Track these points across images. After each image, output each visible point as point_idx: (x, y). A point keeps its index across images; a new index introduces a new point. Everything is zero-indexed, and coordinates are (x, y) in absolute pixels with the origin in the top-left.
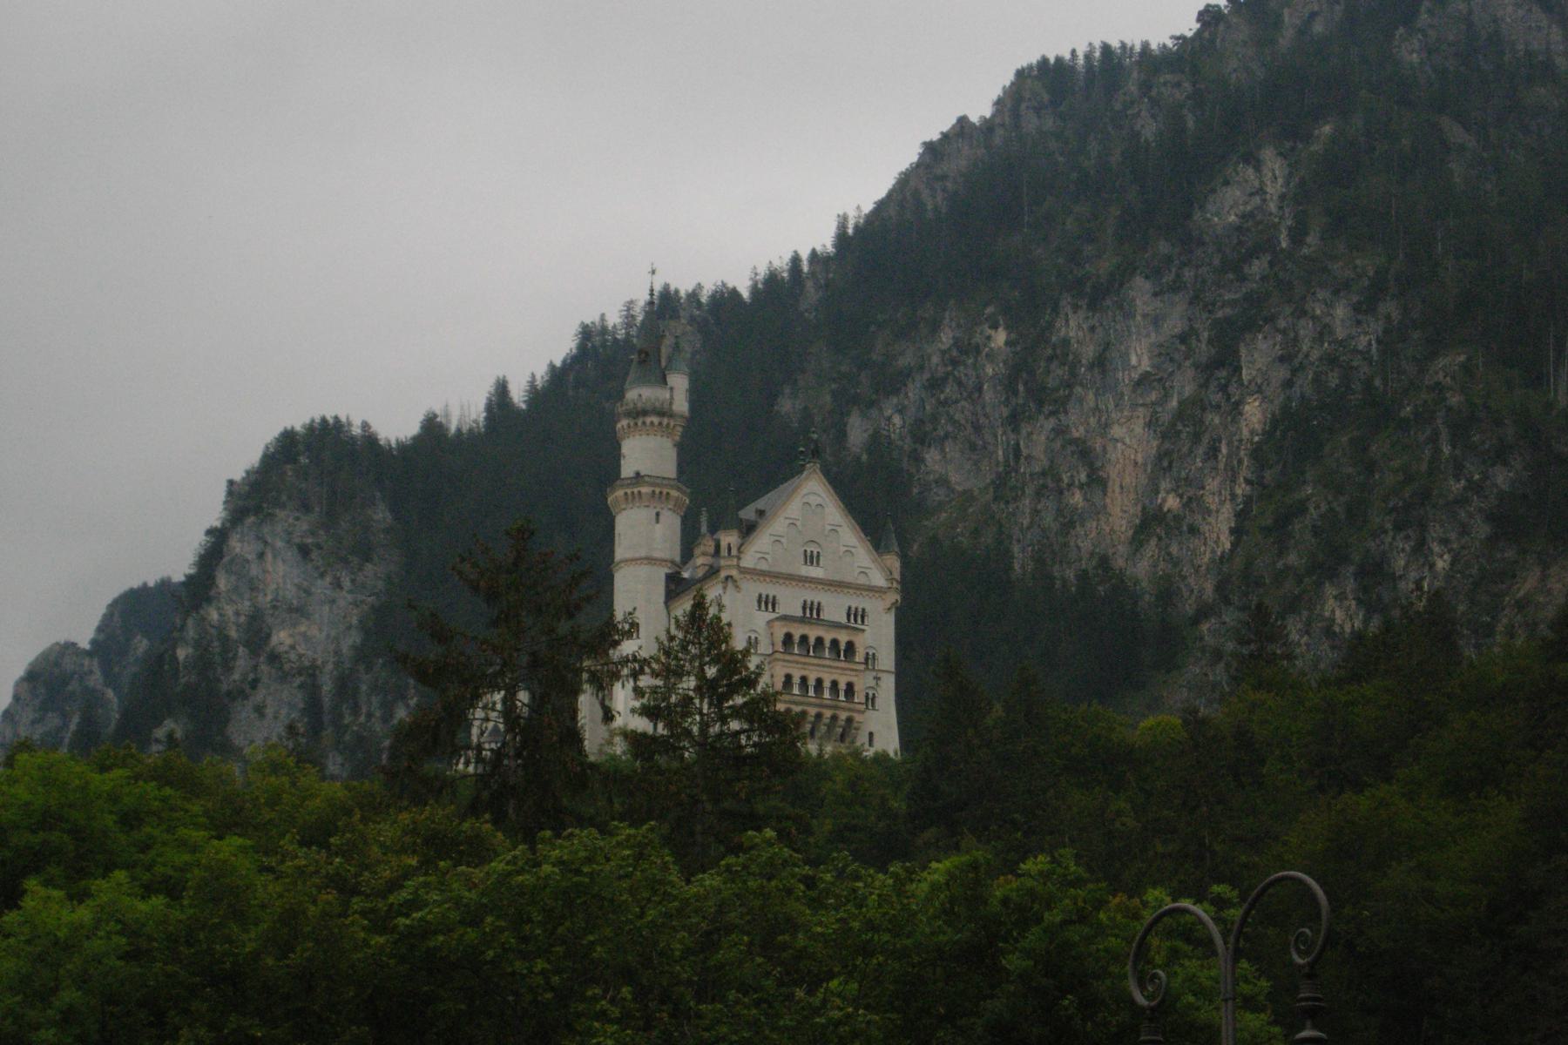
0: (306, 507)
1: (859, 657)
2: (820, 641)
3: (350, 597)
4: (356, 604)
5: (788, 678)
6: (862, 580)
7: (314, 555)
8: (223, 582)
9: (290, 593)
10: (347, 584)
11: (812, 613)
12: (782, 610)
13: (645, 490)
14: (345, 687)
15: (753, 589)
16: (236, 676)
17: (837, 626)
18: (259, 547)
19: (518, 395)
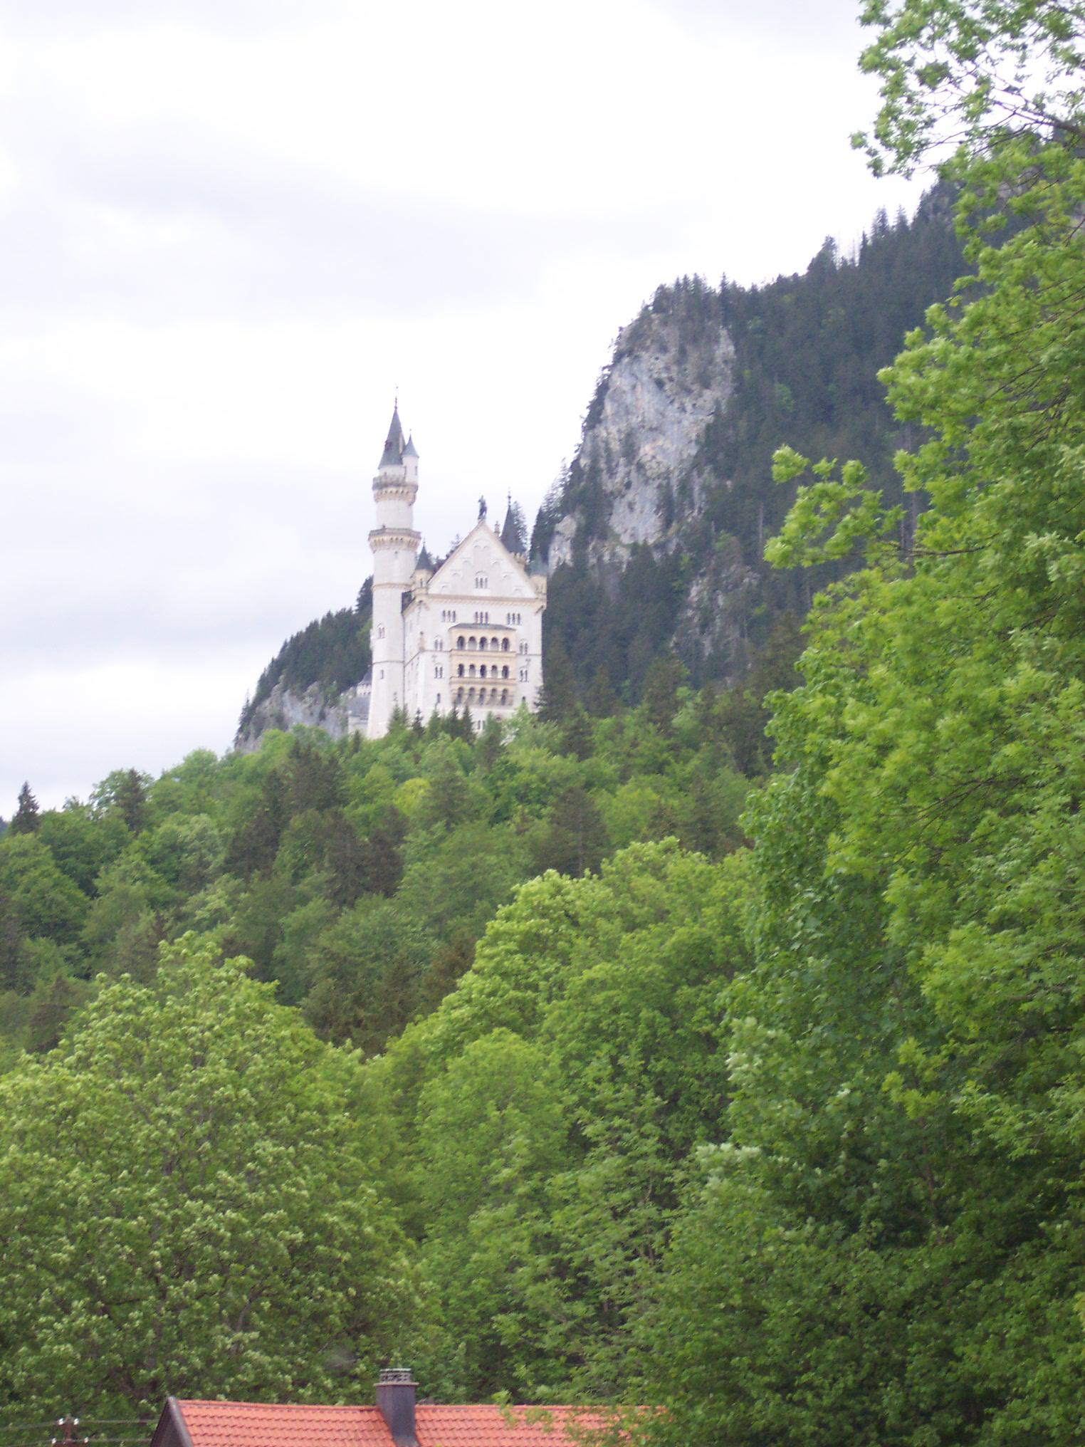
0: (664, 349)
1: (514, 646)
2: (483, 641)
3: (691, 418)
4: (696, 423)
5: (461, 668)
6: (517, 595)
7: (667, 387)
8: (609, 408)
9: (651, 415)
10: (689, 407)
11: (481, 621)
12: (459, 621)
13: (386, 538)
14: (685, 487)
15: (437, 608)
16: (618, 480)
17: (498, 627)
18: (631, 381)
19: (892, 222)
